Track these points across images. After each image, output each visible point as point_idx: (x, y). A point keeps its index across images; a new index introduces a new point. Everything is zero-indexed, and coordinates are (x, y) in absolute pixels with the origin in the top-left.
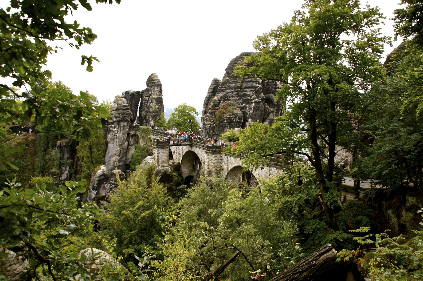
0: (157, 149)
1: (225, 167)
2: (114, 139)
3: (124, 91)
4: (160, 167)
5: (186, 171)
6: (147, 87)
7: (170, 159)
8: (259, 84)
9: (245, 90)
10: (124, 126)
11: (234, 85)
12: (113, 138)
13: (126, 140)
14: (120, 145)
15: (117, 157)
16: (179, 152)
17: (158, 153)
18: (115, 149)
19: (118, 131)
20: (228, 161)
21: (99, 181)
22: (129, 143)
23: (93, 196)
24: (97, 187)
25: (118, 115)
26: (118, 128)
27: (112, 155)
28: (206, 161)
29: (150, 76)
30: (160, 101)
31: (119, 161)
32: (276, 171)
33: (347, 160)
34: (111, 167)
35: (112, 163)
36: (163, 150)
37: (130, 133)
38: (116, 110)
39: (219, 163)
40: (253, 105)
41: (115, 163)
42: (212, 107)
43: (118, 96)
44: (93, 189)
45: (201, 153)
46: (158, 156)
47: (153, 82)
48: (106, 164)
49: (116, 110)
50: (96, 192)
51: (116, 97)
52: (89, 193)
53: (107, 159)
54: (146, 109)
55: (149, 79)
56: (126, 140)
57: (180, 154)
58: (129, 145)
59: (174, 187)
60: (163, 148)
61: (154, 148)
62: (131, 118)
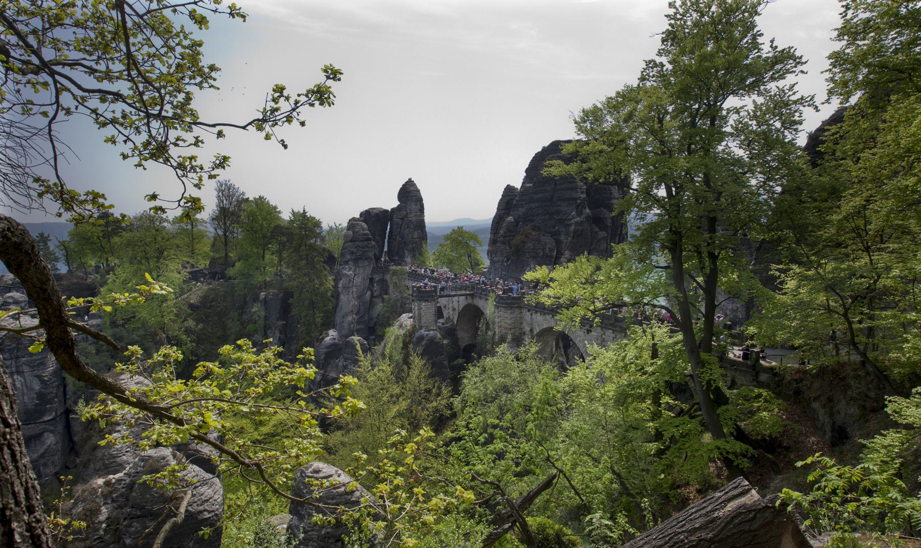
1: (527, 329)
4: (423, 331)
5: (464, 338)
7: (439, 318)
8: (582, 193)
9: (559, 203)
11: (540, 195)
13: (369, 288)
14: (359, 297)
16: (453, 305)
17: (420, 309)
20: (532, 319)
21: (327, 354)
22: (372, 293)
25: (355, 250)
28: (496, 320)
30: (421, 225)
31: (358, 323)
32: (613, 335)
33: (736, 316)
34: (344, 332)
35: (346, 325)
38: (351, 241)
39: (519, 323)
40: (573, 227)
42: (505, 233)
43: (354, 219)
45: (489, 307)
46: (420, 314)
47: (409, 194)
49: (351, 241)
53: (338, 319)
54: (398, 238)
55: (401, 189)
56: (369, 288)
57: (454, 310)
58: (372, 296)
60: (428, 301)
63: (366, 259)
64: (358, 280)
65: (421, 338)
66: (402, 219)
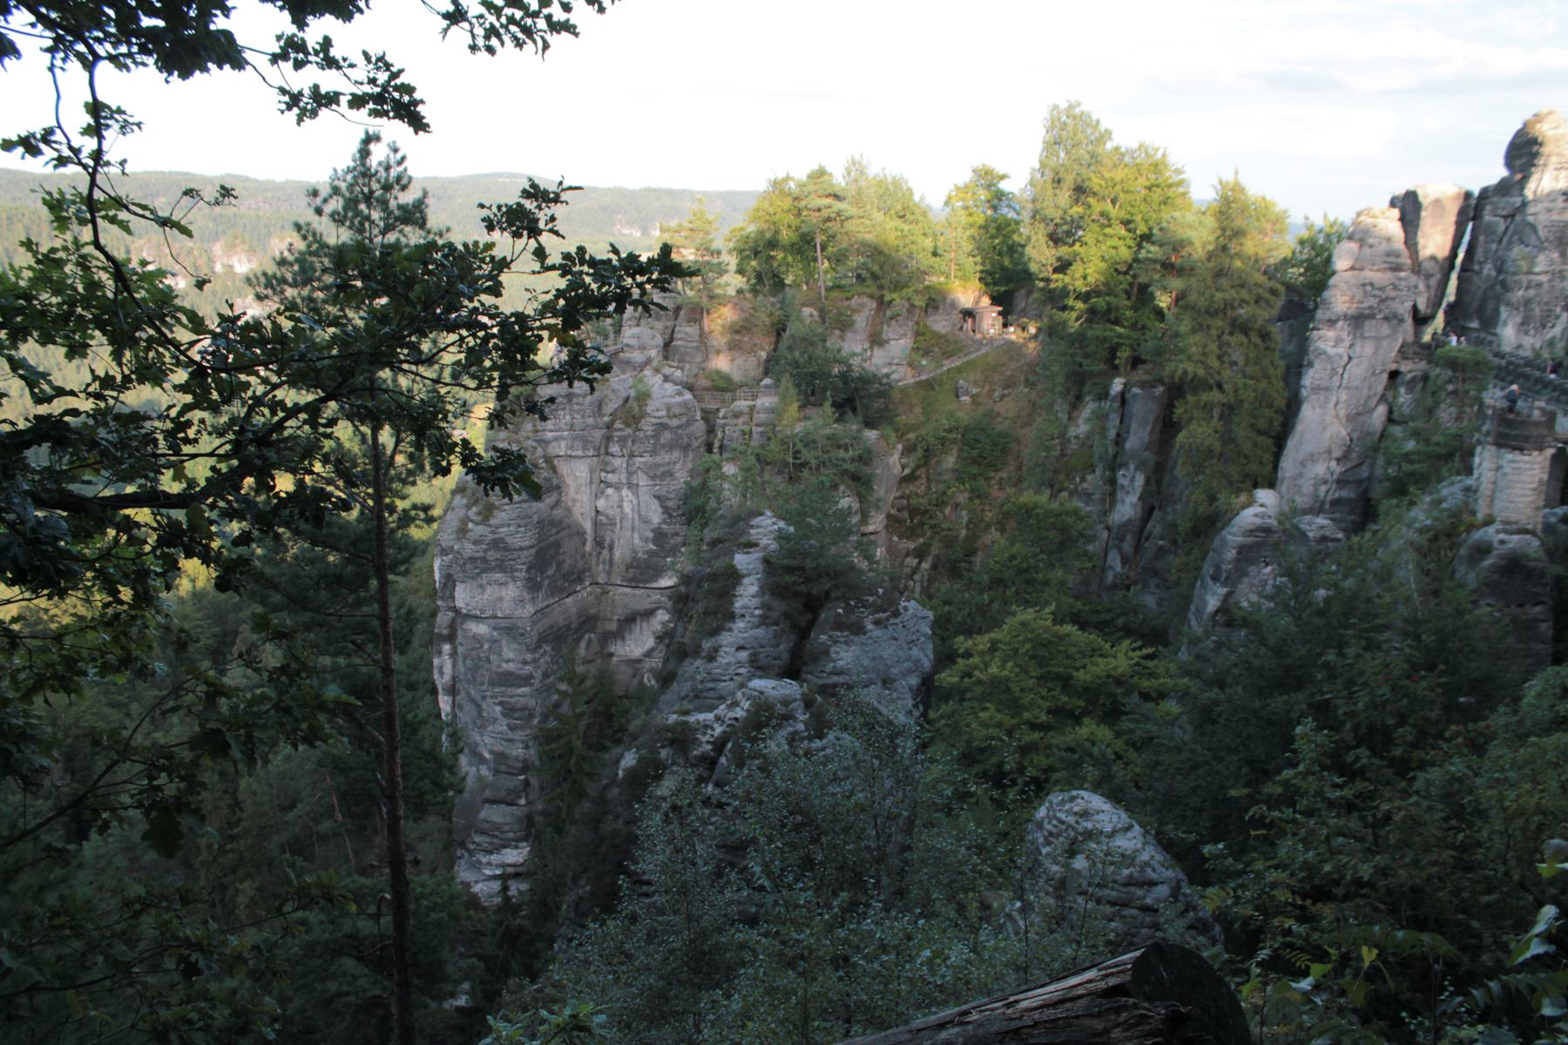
0: (1493, 448)
2: (1327, 389)
3: (1400, 191)
4: (1491, 529)
6: (1504, 173)
10: (1378, 339)
12: (1323, 383)
13: (1383, 398)
14: (1351, 418)
15: (1333, 464)
18: (1328, 433)
19: (1350, 358)
21: (1242, 549)
22: (1391, 411)
23: (1213, 603)
24: (1229, 572)
26: (1352, 345)
27: (1312, 455)
29: (1525, 125)
31: (1341, 482)
35: (1307, 487)
36: (1517, 456)
37: (1403, 369)
38: (1352, 268)
41: (1323, 488)
44: (1215, 578)
47: (1524, 151)
48: (1284, 488)
50: (1224, 590)
51: (1359, 214)
52: (1197, 593)
53: (1288, 464)
58: (1390, 420)
59: (1543, 627)
60: (1521, 450)
61: (1479, 442)
62: (1415, 309)
63: (1386, 319)
64: (1357, 372)
65: (1483, 550)
66: (1510, 217)
